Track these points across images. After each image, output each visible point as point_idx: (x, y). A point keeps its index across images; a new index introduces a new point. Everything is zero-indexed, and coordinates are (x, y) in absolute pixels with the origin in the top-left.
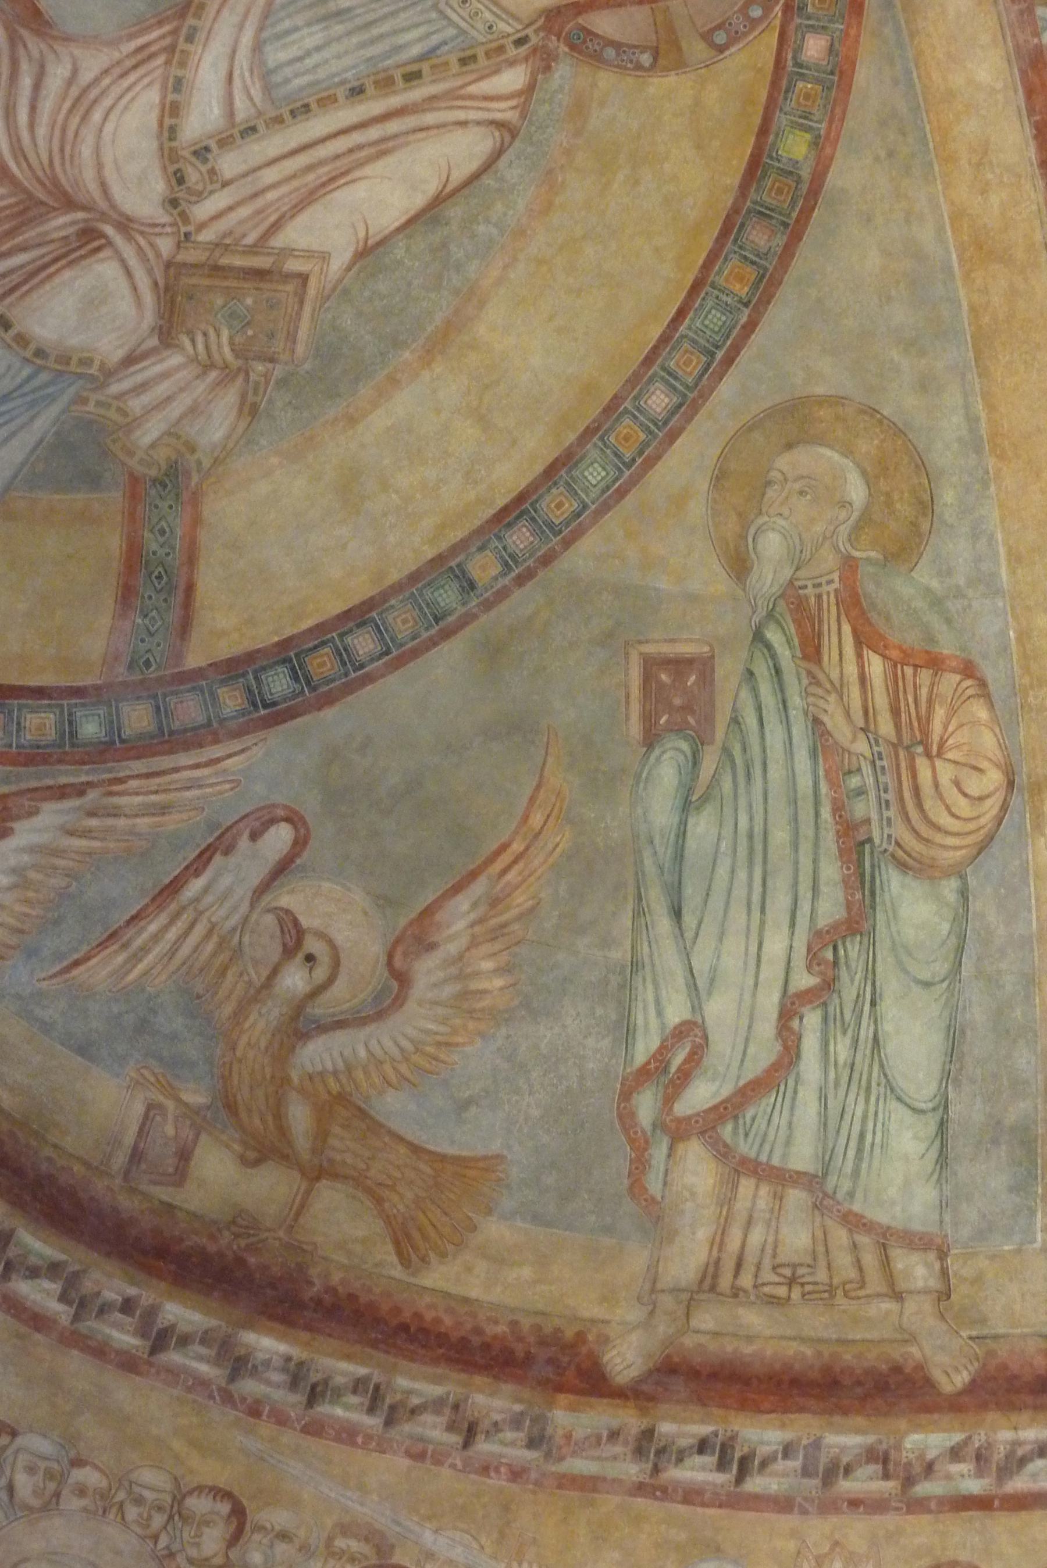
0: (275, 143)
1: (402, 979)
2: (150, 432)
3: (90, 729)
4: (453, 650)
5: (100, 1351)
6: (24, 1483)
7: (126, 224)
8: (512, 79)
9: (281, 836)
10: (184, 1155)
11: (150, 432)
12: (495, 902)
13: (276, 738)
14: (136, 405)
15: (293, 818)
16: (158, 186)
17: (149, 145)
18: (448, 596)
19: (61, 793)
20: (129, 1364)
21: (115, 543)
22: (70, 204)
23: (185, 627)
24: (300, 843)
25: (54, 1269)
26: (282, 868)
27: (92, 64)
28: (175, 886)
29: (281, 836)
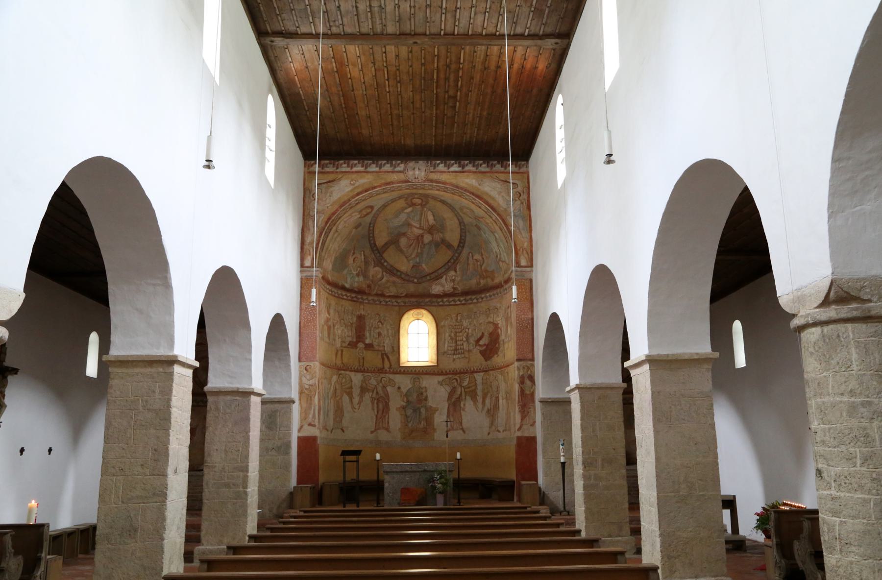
0: (422, 222)
1: (483, 258)
2: (439, 240)
3: (455, 258)
4: (467, 233)
5: (479, 302)
6: (478, 315)
7: (423, 233)
8: (425, 209)
9: (470, 254)
10: (480, 282)
11: (439, 240)
12: (483, 249)
13: (465, 249)
14: (436, 239)
15: (470, 252)
16: (421, 230)
17: (418, 230)
18: (464, 231)
19: (457, 263)
20: (481, 302)
21: (444, 247)
22: (419, 236)
23: (453, 247)
24: (472, 253)
25: (475, 298)
26: (473, 256)
27: (410, 231)
28: (468, 264)
29: (470, 254)
